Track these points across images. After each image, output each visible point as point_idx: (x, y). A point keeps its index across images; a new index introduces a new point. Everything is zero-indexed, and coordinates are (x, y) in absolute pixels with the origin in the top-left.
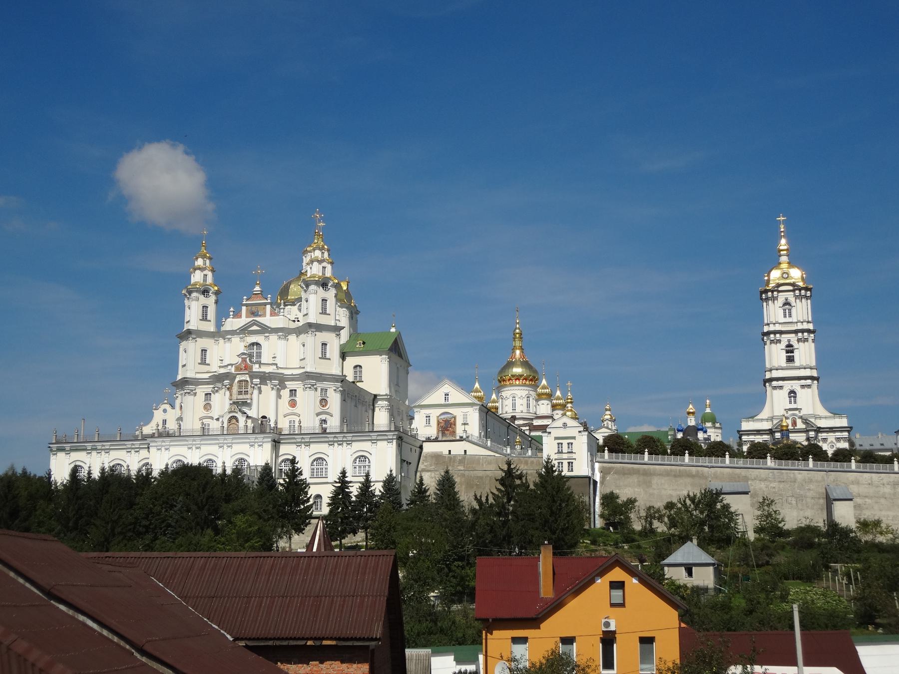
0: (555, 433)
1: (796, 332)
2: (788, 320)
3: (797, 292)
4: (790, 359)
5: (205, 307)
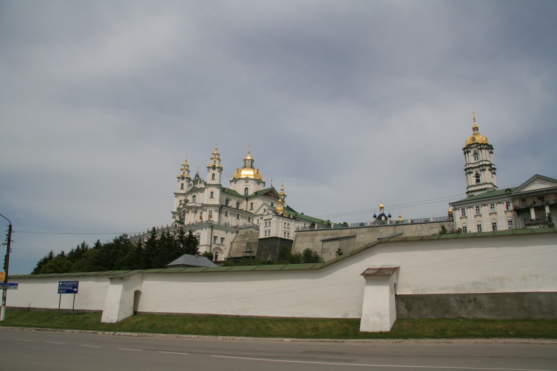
0: (265, 218)
1: (479, 166)
2: (477, 161)
3: (479, 147)
4: (478, 181)
5: (182, 184)
